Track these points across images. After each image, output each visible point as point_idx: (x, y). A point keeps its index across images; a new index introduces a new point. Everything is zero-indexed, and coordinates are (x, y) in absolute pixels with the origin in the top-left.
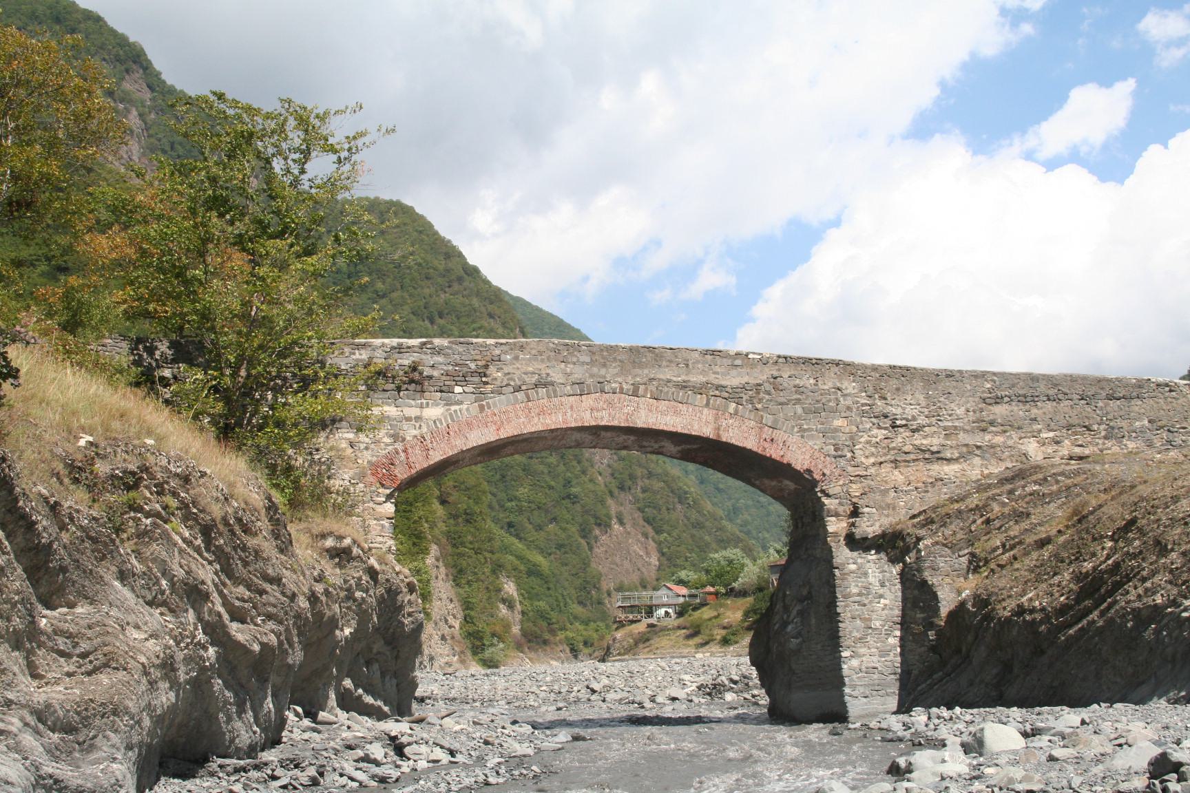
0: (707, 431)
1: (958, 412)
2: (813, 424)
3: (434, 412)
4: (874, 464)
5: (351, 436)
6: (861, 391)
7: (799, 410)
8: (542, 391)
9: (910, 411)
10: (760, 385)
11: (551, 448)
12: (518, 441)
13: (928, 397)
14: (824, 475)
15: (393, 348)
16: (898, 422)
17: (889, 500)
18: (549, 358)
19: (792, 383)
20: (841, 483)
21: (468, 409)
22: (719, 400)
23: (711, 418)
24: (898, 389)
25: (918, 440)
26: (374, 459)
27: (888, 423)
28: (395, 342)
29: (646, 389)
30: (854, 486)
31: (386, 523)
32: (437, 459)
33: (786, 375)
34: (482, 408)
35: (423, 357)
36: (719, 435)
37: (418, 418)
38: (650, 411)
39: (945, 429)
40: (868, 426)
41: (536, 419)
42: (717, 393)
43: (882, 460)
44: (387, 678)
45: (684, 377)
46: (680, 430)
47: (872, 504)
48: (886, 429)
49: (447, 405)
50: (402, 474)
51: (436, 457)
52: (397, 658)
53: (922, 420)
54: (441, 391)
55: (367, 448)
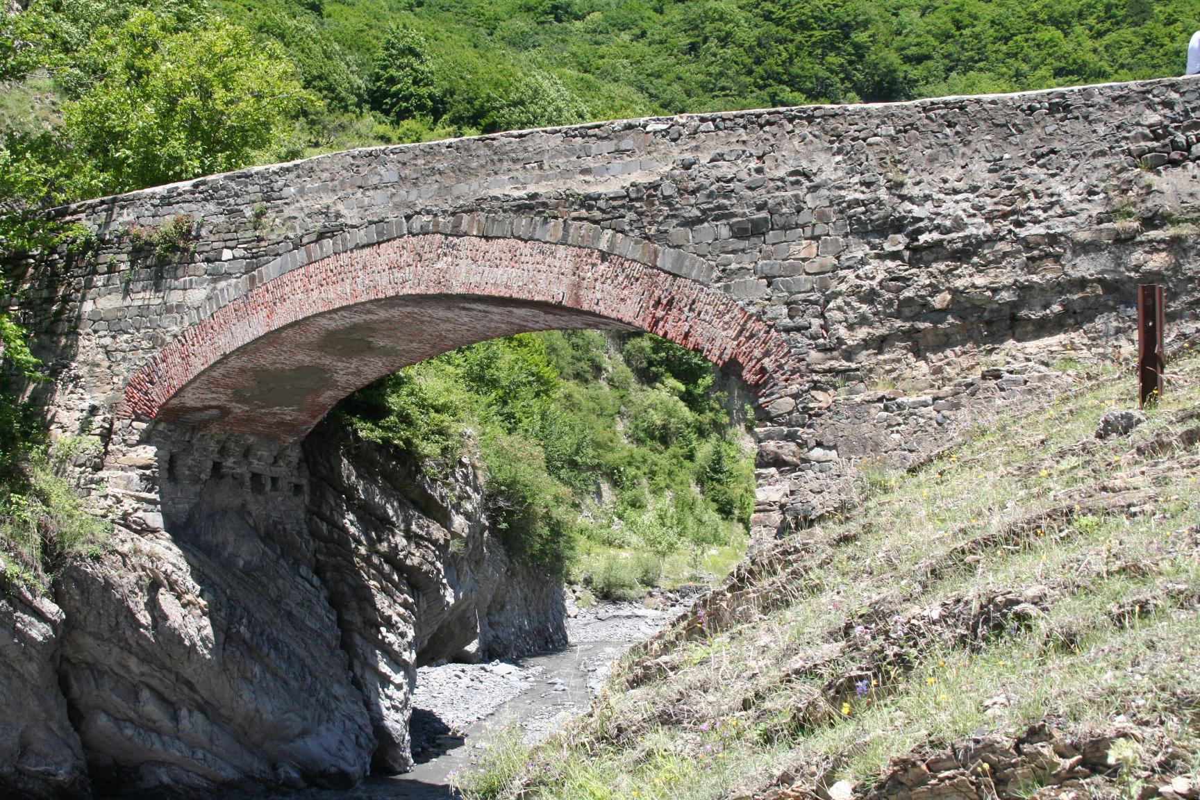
0: (558, 292)
1: (1067, 197)
2: (749, 258)
3: (197, 295)
4: (866, 344)
5: (107, 341)
6: (851, 172)
7: (725, 232)
8: (328, 243)
9: (954, 207)
10: (655, 186)
11: (270, 344)
12: (370, 328)
13: (996, 166)
14: (763, 370)
15: (163, 198)
16: (923, 238)
17: (866, 429)
18: (342, 182)
19: (715, 173)
20: (794, 388)
21: (236, 286)
22: (586, 223)
23: (568, 266)
24: (932, 159)
25: (968, 278)
26: (130, 376)
27: (902, 239)
28: (161, 190)
29: (473, 218)
30: (819, 395)
31: (135, 475)
32: (196, 372)
33: (704, 159)
34: (252, 279)
35: (193, 206)
36: (577, 298)
37: (179, 306)
38: (475, 261)
39: (1027, 244)
40: (860, 254)
41: (316, 292)
42: (584, 213)
43: (883, 331)
44: (184, 713)
45: (532, 189)
46: (515, 296)
47: (829, 438)
48: (895, 256)
49: (215, 281)
50: (158, 395)
51: (198, 366)
52: (189, 684)
53: (978, 228)
54: (208, 260)
55: (124, 359)
